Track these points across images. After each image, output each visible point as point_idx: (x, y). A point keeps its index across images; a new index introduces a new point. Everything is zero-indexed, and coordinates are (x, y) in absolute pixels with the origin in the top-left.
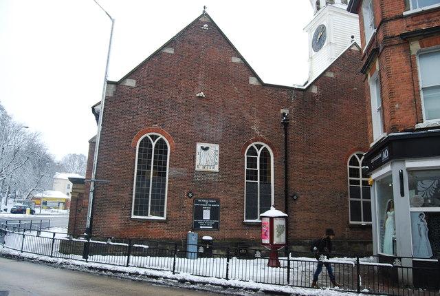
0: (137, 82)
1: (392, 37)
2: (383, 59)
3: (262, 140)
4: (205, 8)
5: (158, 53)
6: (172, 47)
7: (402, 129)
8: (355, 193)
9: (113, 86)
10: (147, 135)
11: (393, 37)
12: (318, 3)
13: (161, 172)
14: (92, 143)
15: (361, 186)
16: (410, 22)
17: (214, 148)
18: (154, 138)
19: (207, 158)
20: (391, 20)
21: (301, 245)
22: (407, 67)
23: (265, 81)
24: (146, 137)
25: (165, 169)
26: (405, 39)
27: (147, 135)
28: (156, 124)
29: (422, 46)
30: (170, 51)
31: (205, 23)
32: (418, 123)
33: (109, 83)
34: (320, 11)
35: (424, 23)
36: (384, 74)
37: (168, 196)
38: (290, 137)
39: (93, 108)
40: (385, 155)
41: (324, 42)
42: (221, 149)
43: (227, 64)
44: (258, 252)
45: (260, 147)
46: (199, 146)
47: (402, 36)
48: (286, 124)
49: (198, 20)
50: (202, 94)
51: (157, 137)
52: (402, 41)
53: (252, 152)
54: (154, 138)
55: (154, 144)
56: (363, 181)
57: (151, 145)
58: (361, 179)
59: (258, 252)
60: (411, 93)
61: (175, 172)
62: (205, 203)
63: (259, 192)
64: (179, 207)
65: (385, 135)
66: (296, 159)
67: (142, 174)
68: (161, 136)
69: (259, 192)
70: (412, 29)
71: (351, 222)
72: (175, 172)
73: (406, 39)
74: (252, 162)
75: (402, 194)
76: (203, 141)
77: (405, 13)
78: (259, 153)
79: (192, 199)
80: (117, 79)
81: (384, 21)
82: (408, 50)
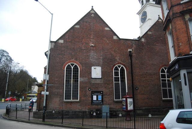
0: (64, 41)
1: (176, 13)
2: (173, 23)
3: (121, 64)
4: (92, 7)
5: (73, 28)
6: (78, 25)
7: (184, 54)
8: (164, 85)
9: (53, 43)
10: (69, 64)
11: (177, 13)
12: (142, 2)
14: (45, 68)
15: (167, 82)
16: (184, 6)
18: (72, 65)
19: (96, 72)
20: (176, 6)
21: (140, 110)
22: (184, 26)
23: (121, 38)
24: (69, 65)
25: (78, 79)
26: (182, 14)
27: (69, 64)
28: (73, 59)
29: (190, 16)
30: (77, 26)
31: (93, 13)
32: (191, 51)
33: (51, 42)
34: (144, 5)
35: (190, 6)
36: (174, 30)
37: (80, 91)
38: (133, 61)
39: (45, 53)
40: (177, 67)
41: (146, 18)
43: (103, 31)
44: (120, 114)
45: (119, 66)
46: (93, 68)
47: (181, 12)
48: (130, 55)
49: (89, 12)
50: (92, 45)
51: (74, 64)
52: (181, 15)
53: (116, 69)
54: (72, 65)
55: (72, 68)
56: (167, 80)
58: (167, 79)
59: (120, 114)
60: (187, 38)
61: (82, 79)
63: (120, 87)
64: (85, 95)
65: (176, 58)
66: (137, 71)
67: (68, 81)
68: (75, 64)
69: (120, 87)
70: (185, 9)
71: (163, 99)
72: (82, 79)
73: (183, 14)
74: (116, 74)
75: (186, 84)
76: (94, 66)
77: (181, 2)
78: (119, 69)
79: (90, 92)
80: (55, 40)
82: (185, 18)
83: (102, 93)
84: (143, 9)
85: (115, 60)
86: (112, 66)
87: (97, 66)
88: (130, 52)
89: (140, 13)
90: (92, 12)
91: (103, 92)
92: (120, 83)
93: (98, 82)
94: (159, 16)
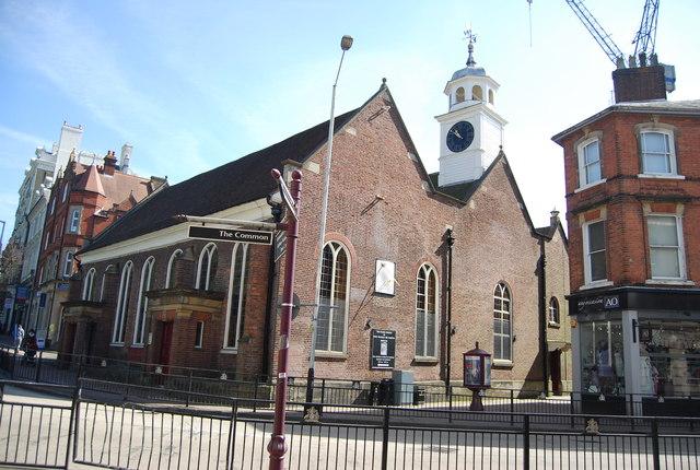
4: (384, 80)
8: (497, 329)
13: (343, 297)
19: (386, 277)
20: (628, 177)
22: (640, 227)
24: (327, 246)
46: (379, 262)
53: (422, 274)
55: (335, 254)
57: (332, 257)
58: (503, 312)
62: (382, 335)
64: (359, 340)
67: (326, 294)
73: (639, 198)
74: (422, 284)
76: (381, 258)
77: (640, 176)
81: (619, 177)
85: (422, 250)
86: (415, 264)
94: (501, 147)
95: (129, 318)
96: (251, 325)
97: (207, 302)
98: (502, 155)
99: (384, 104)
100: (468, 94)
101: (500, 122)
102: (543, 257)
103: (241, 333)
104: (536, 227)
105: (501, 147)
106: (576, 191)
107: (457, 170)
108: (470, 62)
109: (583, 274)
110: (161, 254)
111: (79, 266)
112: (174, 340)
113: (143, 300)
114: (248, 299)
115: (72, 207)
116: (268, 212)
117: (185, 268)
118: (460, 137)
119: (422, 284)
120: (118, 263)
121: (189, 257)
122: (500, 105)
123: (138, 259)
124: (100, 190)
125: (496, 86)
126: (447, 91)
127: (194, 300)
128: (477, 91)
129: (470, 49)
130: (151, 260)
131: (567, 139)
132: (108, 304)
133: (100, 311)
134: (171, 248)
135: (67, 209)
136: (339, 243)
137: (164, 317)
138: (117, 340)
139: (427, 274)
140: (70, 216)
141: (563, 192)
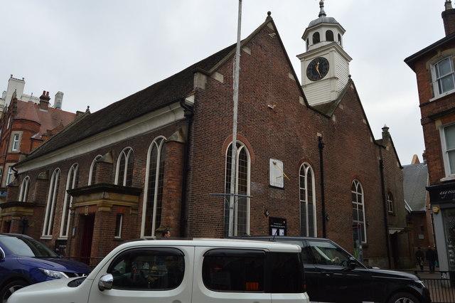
4: (269, 13)
17: (280, 164)
41: (325, 74)
42: (285, 167)
43: (286, 79)
45: (306, 166)
48: (321, 146)
53: (303, 173)
58: (358, 203)
66: (326, 181)
76: (273, 157)
83: (285, 225)
84: (322, 51)
86: (297, 163)
87: (277, 158)
88: (320, 138)
89: (305, 58)
90: (270, 26)
91: (285, 220)
92: (307, 203)
93: (279, 195)
95: (56, 214)
96: (168, 215)
97: (125, 197)
98: (351, 82)
99: (267, 34)
100: (323, 37)
101: (347, 59)
102: (381, 162)
103: (158, 225)
104: (376, 139)
105: (350, 76)
106: (431, 100)
107: (318, 94)
108: (322, 14)
109: (443, 168)
110: (83, 161)
111: (17, 175)
112: (96, 232)
113: (69, 199)
114: (165, 191)
115: (14, 133)
116: (181, 115)
117: (109, 167)
118: (318, 69)
119: (302, 179)
120: (48, 170)
121: (107, 158)
122: (348, 44)
123: (64, 166)
124: (36, 119)
125: (342, 31)
126: (305, 37)
127: (114, 196)
128: (329, 36)
129: (321, 5)
130: (75, 166)
131: (415, 62)
132: (39, 206)
133: (31, 211)
134: (93, 154)
135: (10, 134)
136: (241, 143)
137: (86, 211)
138: (46, 234)
139: (306, 170)
140: (11, 139)
141: (418, 103)
